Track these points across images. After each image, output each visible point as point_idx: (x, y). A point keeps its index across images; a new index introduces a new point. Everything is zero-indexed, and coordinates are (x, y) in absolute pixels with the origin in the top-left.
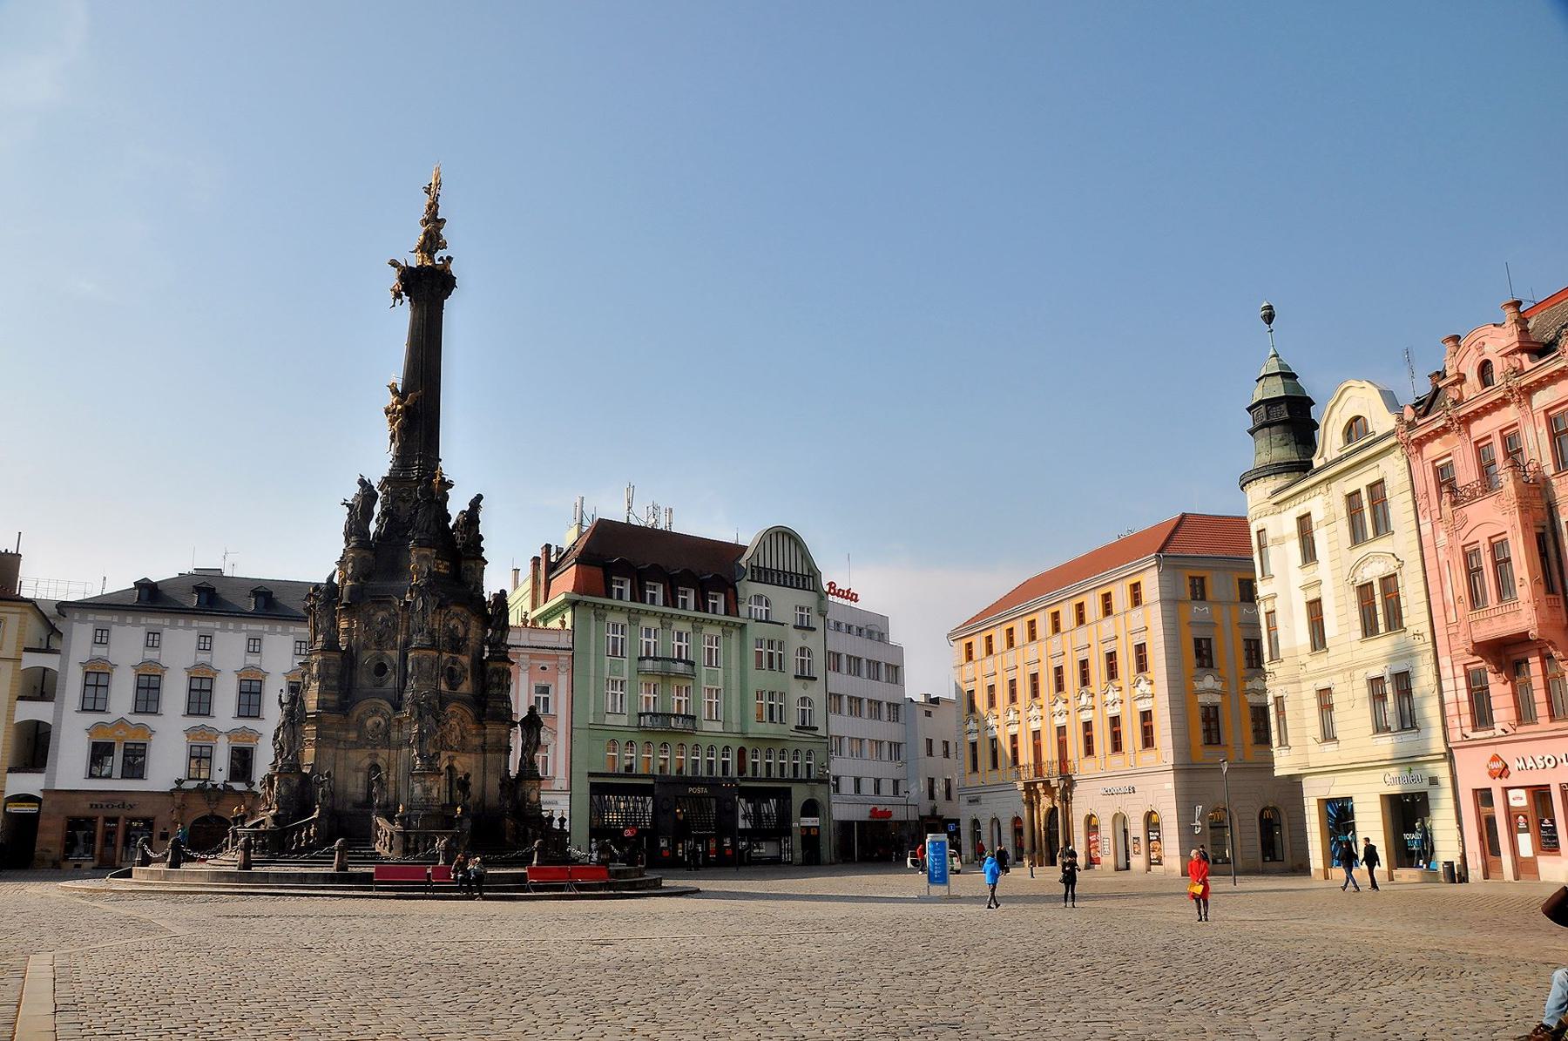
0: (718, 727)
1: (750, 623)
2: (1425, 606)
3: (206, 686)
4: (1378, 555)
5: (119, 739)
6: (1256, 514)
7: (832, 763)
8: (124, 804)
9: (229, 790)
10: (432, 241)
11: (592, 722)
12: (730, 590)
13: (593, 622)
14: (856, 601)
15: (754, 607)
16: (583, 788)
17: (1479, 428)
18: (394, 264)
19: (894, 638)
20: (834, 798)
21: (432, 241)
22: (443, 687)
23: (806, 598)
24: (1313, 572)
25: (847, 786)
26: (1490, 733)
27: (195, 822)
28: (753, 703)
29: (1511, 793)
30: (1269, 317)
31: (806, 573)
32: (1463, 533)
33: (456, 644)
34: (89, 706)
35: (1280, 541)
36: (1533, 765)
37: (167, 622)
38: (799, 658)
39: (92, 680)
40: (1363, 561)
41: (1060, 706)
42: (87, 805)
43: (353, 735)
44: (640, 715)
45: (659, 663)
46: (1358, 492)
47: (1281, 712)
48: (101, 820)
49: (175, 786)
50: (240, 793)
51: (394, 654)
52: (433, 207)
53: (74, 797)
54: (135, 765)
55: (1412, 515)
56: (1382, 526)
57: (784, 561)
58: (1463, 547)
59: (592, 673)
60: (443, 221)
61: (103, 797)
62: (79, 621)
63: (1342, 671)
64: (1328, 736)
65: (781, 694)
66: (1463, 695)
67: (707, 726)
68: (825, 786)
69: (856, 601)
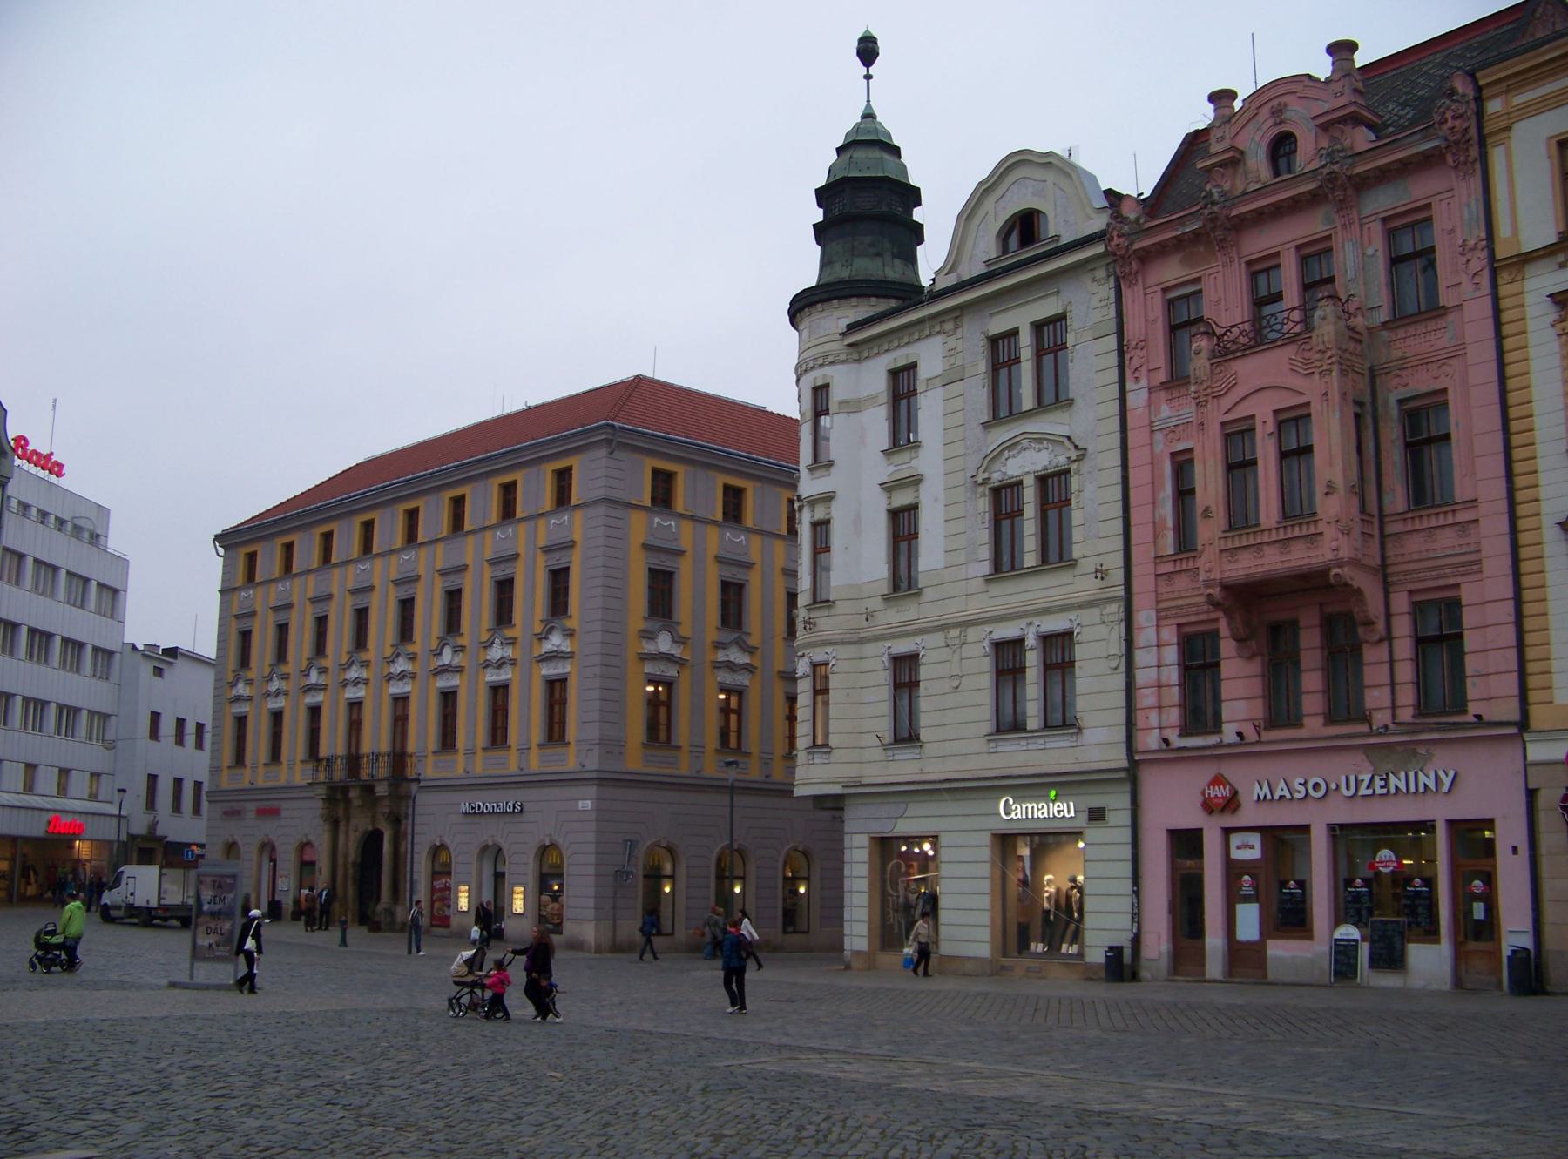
2: (1118, 526)
4: (1040, 440)
6: (815, 360)
14: (59, 475)
17: (1258, 243)
19: (116, 542)
24: (904, 465)
26: (1212, 740)
29: (1235, 839)
30: (868, 51)
32: (1227, 402)
35: (854, 406)
36: (1286, 793)
40: (1011, 446)
41: (401, 665)
46: (1014, 333)
47: (821, 691)
55: (1113, 375)
56: (1053, 397)
58: (1223, 424)
63: (944, 628)
64: (906, 735)
66: (1172, 675)
69: (59, 475)
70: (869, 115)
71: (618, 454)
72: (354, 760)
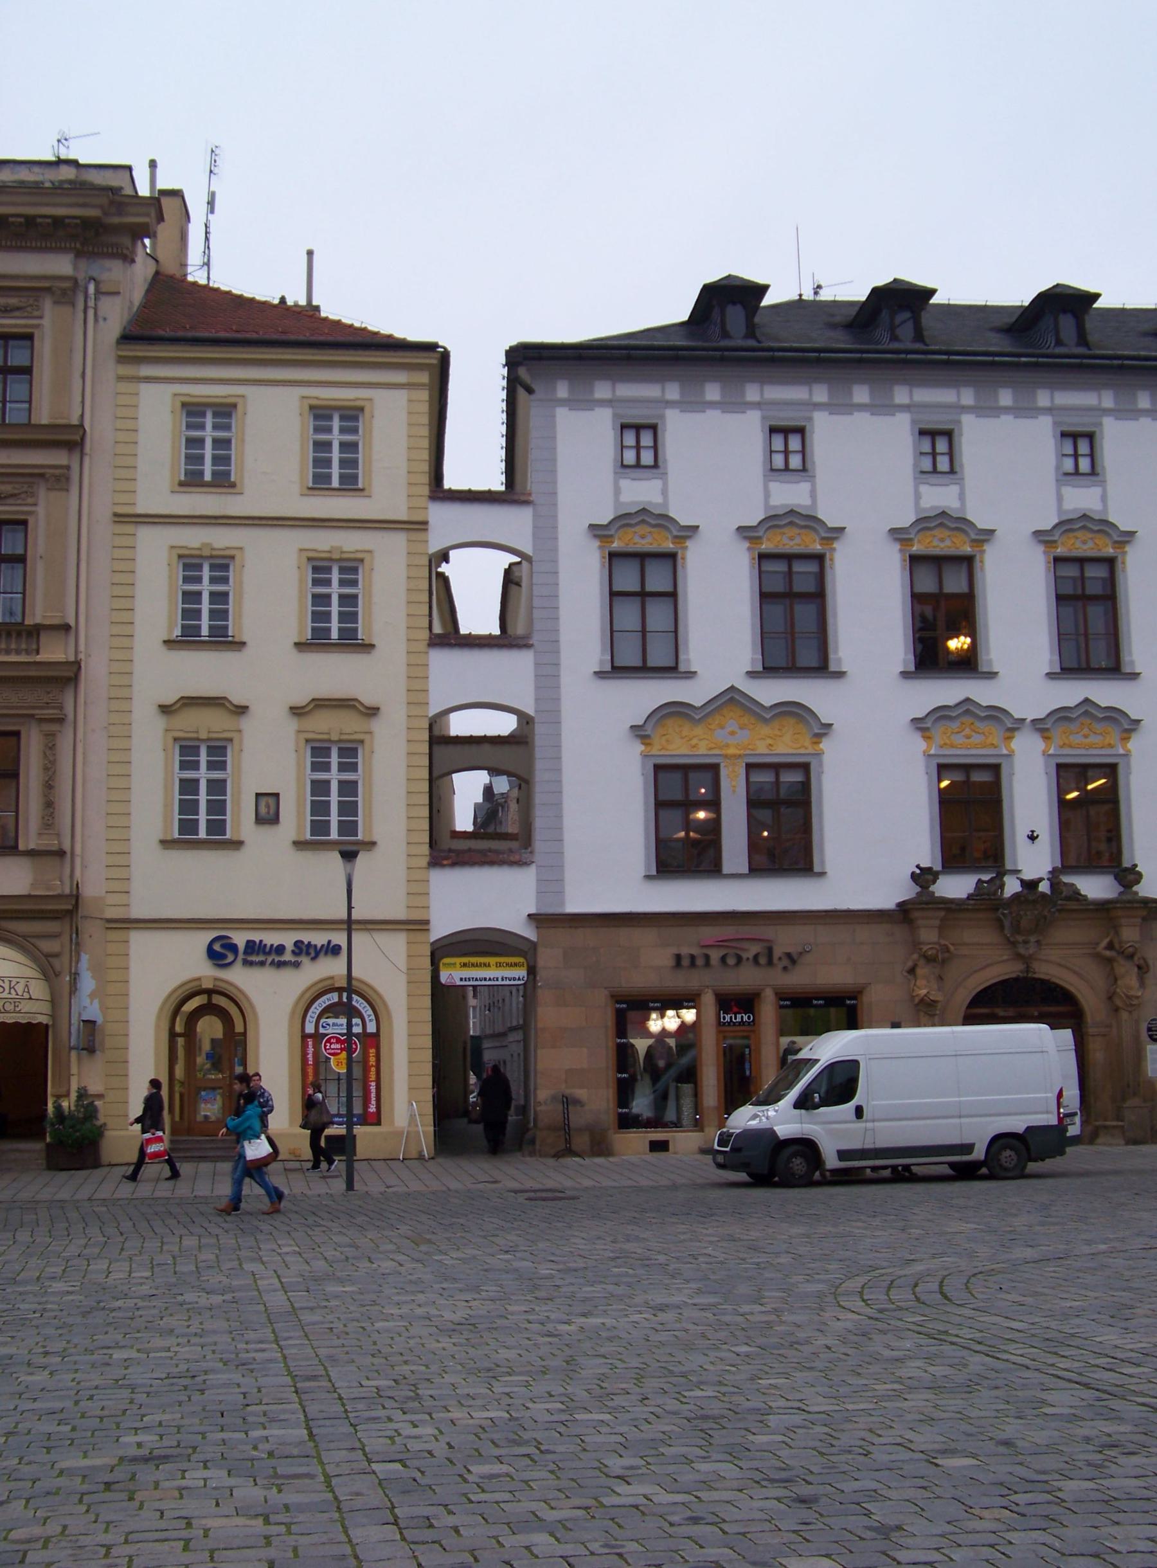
3: (954, 584)
8: (770, 951)
9: (1068, 898)
42: (663, 958)
50: (1103, 908)
53: (624, 935)
61: (710, 933)
62: (573, 403)
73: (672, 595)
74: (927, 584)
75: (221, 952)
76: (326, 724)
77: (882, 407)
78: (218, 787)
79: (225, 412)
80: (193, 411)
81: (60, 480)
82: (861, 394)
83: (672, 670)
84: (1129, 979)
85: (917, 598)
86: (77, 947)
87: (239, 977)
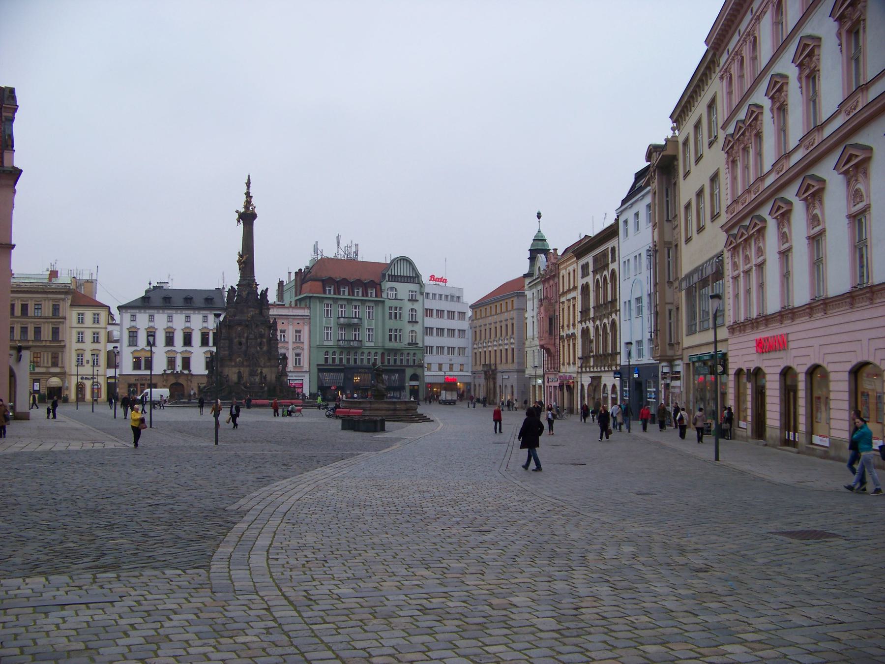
0: (372, 344)
1: (387, 301)
3: (171, 335)
5: (143, 356)
7: (426, 359)
10: (248, 203)
11: (318, 344)
12: (378, 286)
13: (318, 304)
15: (389, 292)
16: (315, 371)
18: (237, 212)
20: (426, 373)
21: (248, 203)
22: (258, 348)
23: (414, 287)
25: (435, 367)
27: (172, 385)
28: (387, 333)
30: (539, 216)
31: (414, 276)
33: (262, 336)
34: (131, 344)
37: (156, 311)
38: (410, 313)
39: (131, 334)
43: (233, 364)
44: (338, 340)
45: (346, 319)
48: (139, 385)
49: (163, 372)
50: (186, 374)
51: (244, 340)
52: (248, 194)
54: (149, 365)
57: (405, 271)
59: (318, 325)
60: (252, 197)
65: (400, 330)
67: (368, 344)
68: (421, 369)
70: (539, 232)
71: (520, 298)
72: (490, 365)
73: (136, 336)
74: (168, 335)
75: (82, 378)
76: (94, 352)
77: (163, 313)
78: (82, 359)
79: (83, 314)
80: (79, 314)
81: (63, 323)
82: (161, 311)
83: (136, 345)
84: (189, 382)
85: (166, 337)
86: (65, 377)
87: (84, 381)
